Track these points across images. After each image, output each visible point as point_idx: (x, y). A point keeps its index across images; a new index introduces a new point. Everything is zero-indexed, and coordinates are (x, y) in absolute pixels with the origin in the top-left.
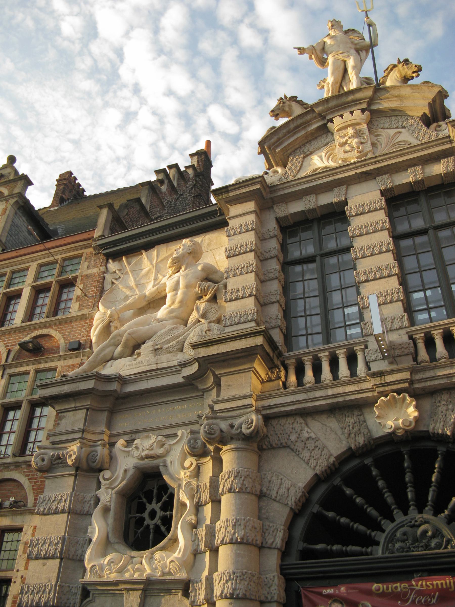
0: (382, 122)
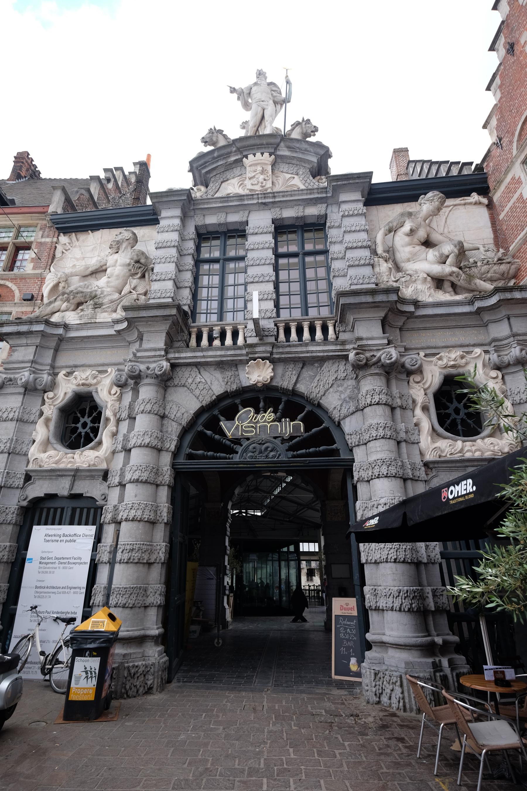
0: (282, 167)
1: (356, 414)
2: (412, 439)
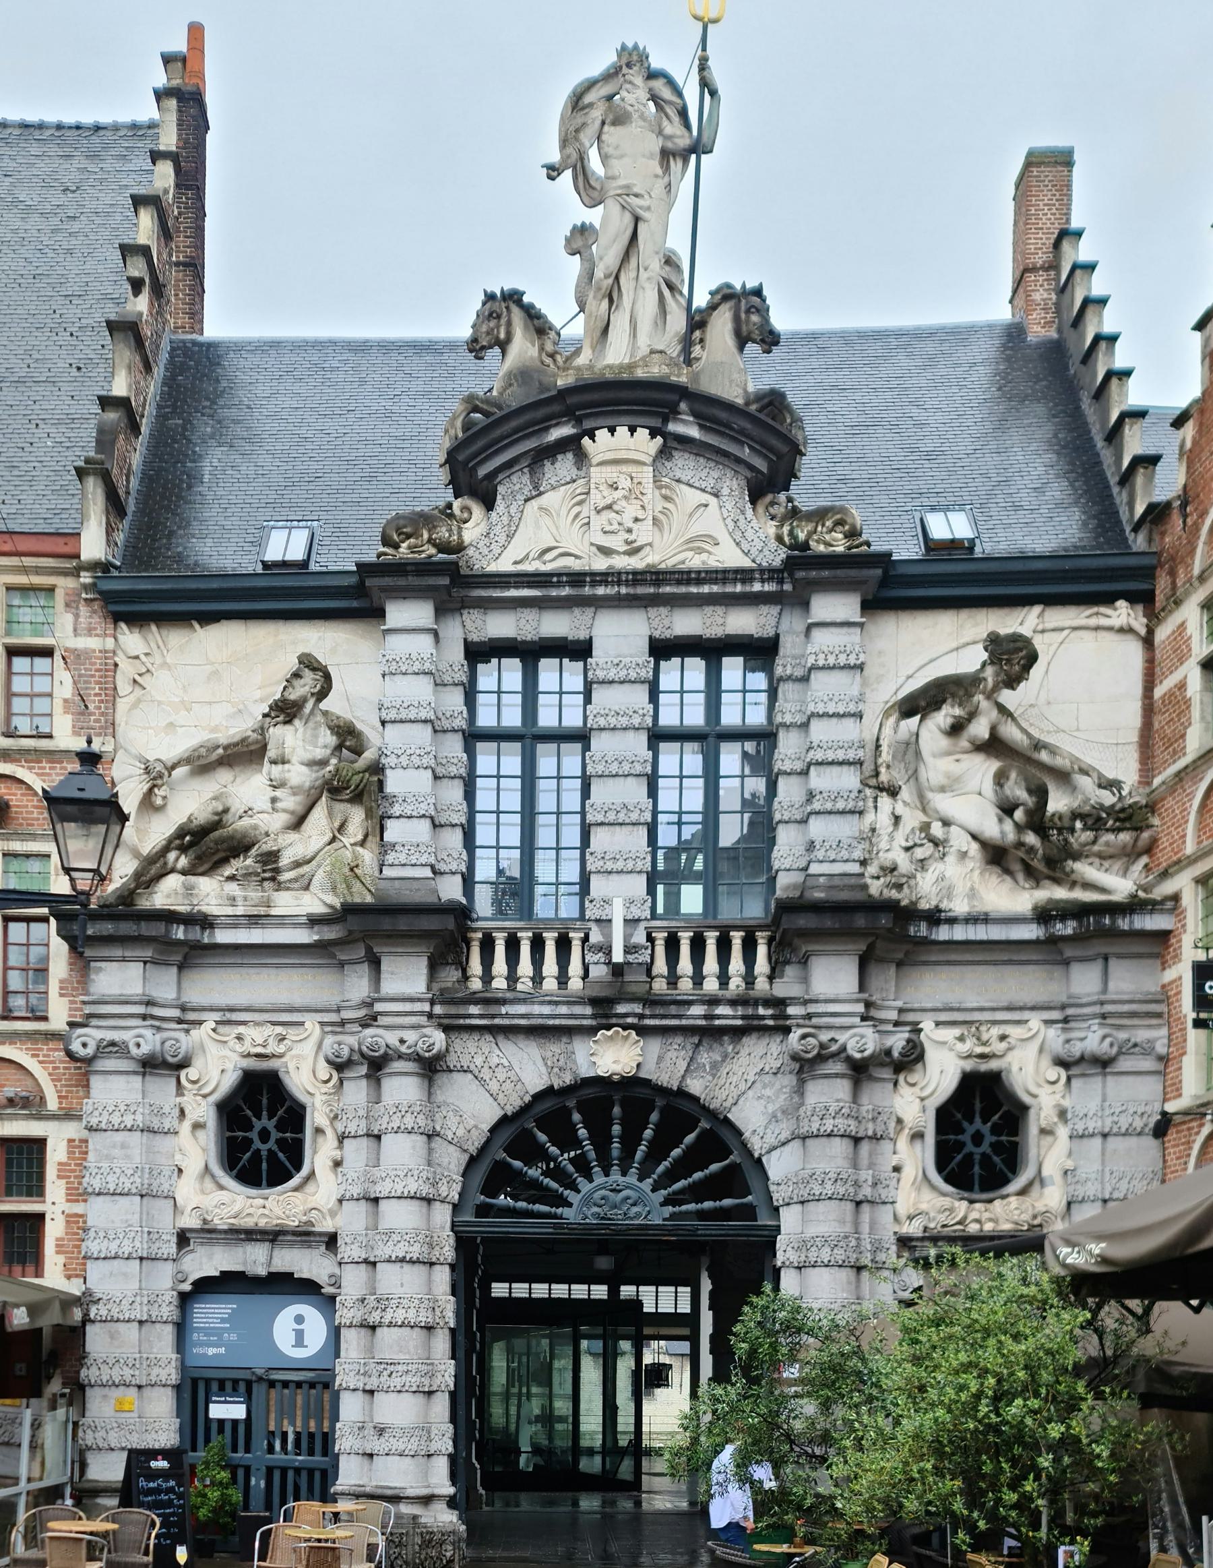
0: (680, 463)
1: (791, 1144)
2: (883, 1197)
